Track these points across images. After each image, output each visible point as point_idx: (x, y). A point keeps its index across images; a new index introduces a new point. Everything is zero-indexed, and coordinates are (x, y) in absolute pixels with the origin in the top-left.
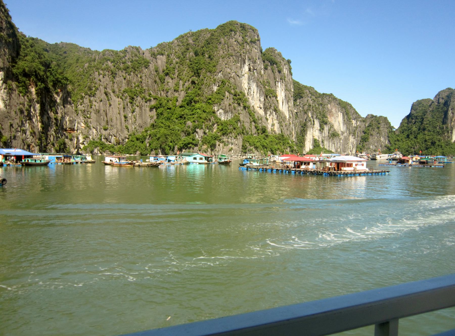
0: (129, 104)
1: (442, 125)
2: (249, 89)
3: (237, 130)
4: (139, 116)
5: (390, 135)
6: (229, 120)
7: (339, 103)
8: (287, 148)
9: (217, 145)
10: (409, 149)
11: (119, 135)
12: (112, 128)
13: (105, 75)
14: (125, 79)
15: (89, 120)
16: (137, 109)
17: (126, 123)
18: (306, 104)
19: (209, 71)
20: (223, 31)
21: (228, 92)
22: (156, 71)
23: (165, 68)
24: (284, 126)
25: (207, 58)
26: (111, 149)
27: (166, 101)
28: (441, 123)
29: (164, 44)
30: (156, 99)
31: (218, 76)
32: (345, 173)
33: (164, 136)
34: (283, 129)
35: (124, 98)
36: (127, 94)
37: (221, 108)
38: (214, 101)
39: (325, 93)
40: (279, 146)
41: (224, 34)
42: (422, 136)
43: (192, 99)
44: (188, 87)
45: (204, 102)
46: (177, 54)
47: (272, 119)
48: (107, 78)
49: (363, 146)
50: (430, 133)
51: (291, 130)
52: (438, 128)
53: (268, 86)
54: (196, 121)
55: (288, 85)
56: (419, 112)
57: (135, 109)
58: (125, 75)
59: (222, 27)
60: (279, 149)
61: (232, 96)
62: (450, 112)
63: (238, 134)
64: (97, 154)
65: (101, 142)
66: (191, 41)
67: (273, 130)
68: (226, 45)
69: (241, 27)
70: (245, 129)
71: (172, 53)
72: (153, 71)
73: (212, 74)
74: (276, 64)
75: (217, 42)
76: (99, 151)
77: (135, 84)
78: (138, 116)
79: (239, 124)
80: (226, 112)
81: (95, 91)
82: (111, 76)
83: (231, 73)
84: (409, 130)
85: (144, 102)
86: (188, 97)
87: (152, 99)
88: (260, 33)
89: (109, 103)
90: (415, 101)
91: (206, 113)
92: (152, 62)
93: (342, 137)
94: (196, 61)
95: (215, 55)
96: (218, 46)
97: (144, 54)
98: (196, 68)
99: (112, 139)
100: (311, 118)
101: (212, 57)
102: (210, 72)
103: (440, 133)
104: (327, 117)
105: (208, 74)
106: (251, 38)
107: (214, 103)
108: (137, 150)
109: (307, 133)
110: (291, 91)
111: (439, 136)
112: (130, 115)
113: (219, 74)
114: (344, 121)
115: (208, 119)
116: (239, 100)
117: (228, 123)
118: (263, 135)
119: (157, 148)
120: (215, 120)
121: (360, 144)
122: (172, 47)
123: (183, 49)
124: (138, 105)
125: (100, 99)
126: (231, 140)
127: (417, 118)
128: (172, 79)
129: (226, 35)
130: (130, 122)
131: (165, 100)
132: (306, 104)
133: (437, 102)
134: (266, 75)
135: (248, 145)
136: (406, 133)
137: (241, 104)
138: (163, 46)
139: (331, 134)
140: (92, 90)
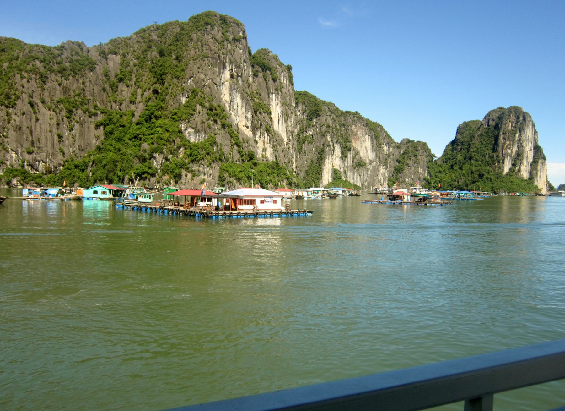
0: (65, 119)
2: (231, 101)
3: (212, 156)
4: (79, 136)
5: (430, 164)
6: (201, 142)
7: (367, 124)
8: (282, 181)
9: (184, 176)
10: (453, 182)
11: (51, 160)
12: (39, 151)
13: (31, 79)
14: (60, 85)
15: (6, 140)
16: (77, 126)
17: (61, 145)
18: (324, 125)
19: (176, 77)
20: (196, 24)
21: (200, 104)
22: (106, 76)
23: (119, 72)
24: (279, 151)
25: (174, 59)
26: (38, 180)
27: (118, 116)
28: (491, 151)
29: (118, 40)
30: (105, 112)
31: (187, 84)
32: (225, 213)
33: (112, 163)
34: (279, 156)
35: (58, 111)
36: (62, 105)
37: (190, 127)
38: (180, 117)
39: (348, 110)
40: (271, 178)
41: (196, 28)
42: (468, 167)
43: (152, 114)
44: (148, 97)
45: (168, 118)
46: (136, 54)
47: (264, 142)
48: (33, 82)
49: (397, 179)
50: (477, 163)
51: (291, 157)
52: (487, 156)
53: (258, 99)
54: (155, 144)
55: (287, 98)
56: (465, 137)
57: (74, 125)
58: (60, 80)
59: (195, 19)
60: (271, 181)
61: (205, 111)
62: (501, 137)
63: (213, 161)
64: (17, 186)
65: (22, 170)
66: (154, 37)
67: (264, 157)
68: (199, 43)
69: (221, 20)
70: (224, 154)
71: (129, 52)
72: (101, 75)
73: (180, 81)
74: (270, 70)
75: (187, 39)
76: (20, 182)
77: (74, 92)
78: (77, 135)
79: (215, 148)
80: (197, 131)
81: (15, 100)
82: (40, 79)
83: (205, 80)
84: (453, 159)
85: (88, 117)
86: (147, 111)
87: (99, 112)
88: (246, 28)
89: (36, 117)
90: (461, 123)
91: (169, 133)
92: (99, 64)
93: (370, 167)
94: (160, 64)
95: (184, 55)
96: (189, 44)
97: (88, 52)
98: (159, 72)
99: (40, 166)
100: (330, 143)
101: (180, 58)
102: (177, 78)
103: (489, 163)
104: (350, 142)
105: (175, 80)
106: (234, 34)
107: (180, 119)
108: (76, 181)
109: (325, 162)
110: (291, 105)
111: (488, 167)
112: (67, 134)
113: (189, 81)
114: (373, 146)
115: (171, 140)
116: (215, 116)
117: (199, 147)
118: (250, 163)
119: (102, 178)
120: (181, 142)
121: (393, 176)
122: (130, 44)
123: (144, 46)
124: (79, 120)
125: (22, 112)
126: (204, 169)
127: (463, 145)
128: (128, 87)
129: (199, 29)
130: (67, 143)
131: (117, 114)
132: (324, 125)
133: (487, 124)
134: (256, 84)
135: (226, 175)
136: (450, 163)
137: (219, 122)
138: (117, 43)
139: (356, 163)
140: (11, 98)
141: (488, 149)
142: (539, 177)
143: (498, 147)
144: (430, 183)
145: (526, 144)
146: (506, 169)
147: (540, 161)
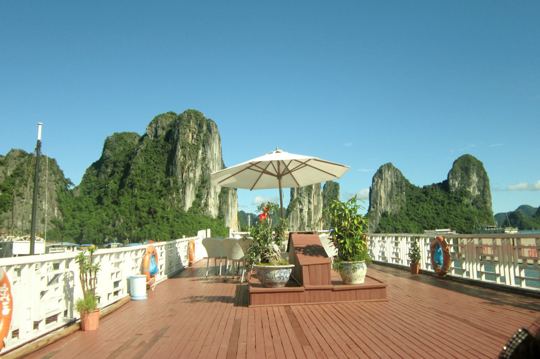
1: (166, 177)
10: (104, 226)
50: (143, 193)
62: (179, 153)
84: (101, 188)
90: (111, 134)
111: (162, 199)
133: (153, 134)
136: (95, 194)
143: (176, 168)
144: (62, 229)
145: (213, 166)
146: (189, 204)
147: (230, 191)
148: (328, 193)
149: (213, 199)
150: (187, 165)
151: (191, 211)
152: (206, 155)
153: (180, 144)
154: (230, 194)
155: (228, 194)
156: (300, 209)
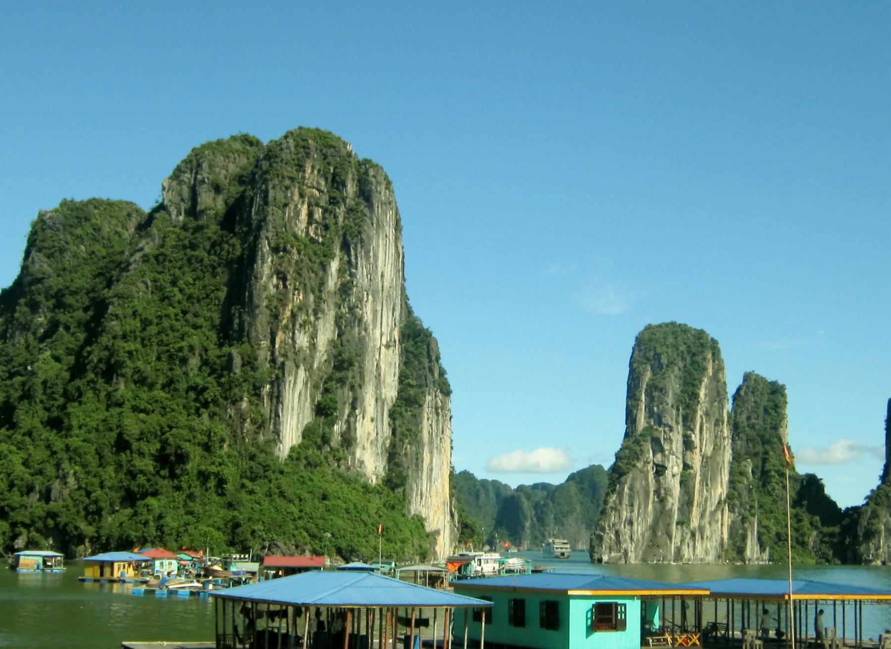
1: (220, 346)
10: (15, 498)
28: (214, 337)
50: (144, 394)
52: (194, 362)
62: (265, 267)
84: (11, 376)
90: (51, 204)
103: (208, 395)
111: (205, 416)
127: (60, 305)
133: (183, 206)
141: (196, 327)
142: (424, 477)
143: (253, 316)
145: (375, 312)
147: (429, 398)
148: (749, 418)
149: (372, 420)
150: (290, 307)
151: (298, 459)
152: (352, 275)
153: (267, 238)
154: (426, 406)
155: (421, 406)
156: (657, 465)
